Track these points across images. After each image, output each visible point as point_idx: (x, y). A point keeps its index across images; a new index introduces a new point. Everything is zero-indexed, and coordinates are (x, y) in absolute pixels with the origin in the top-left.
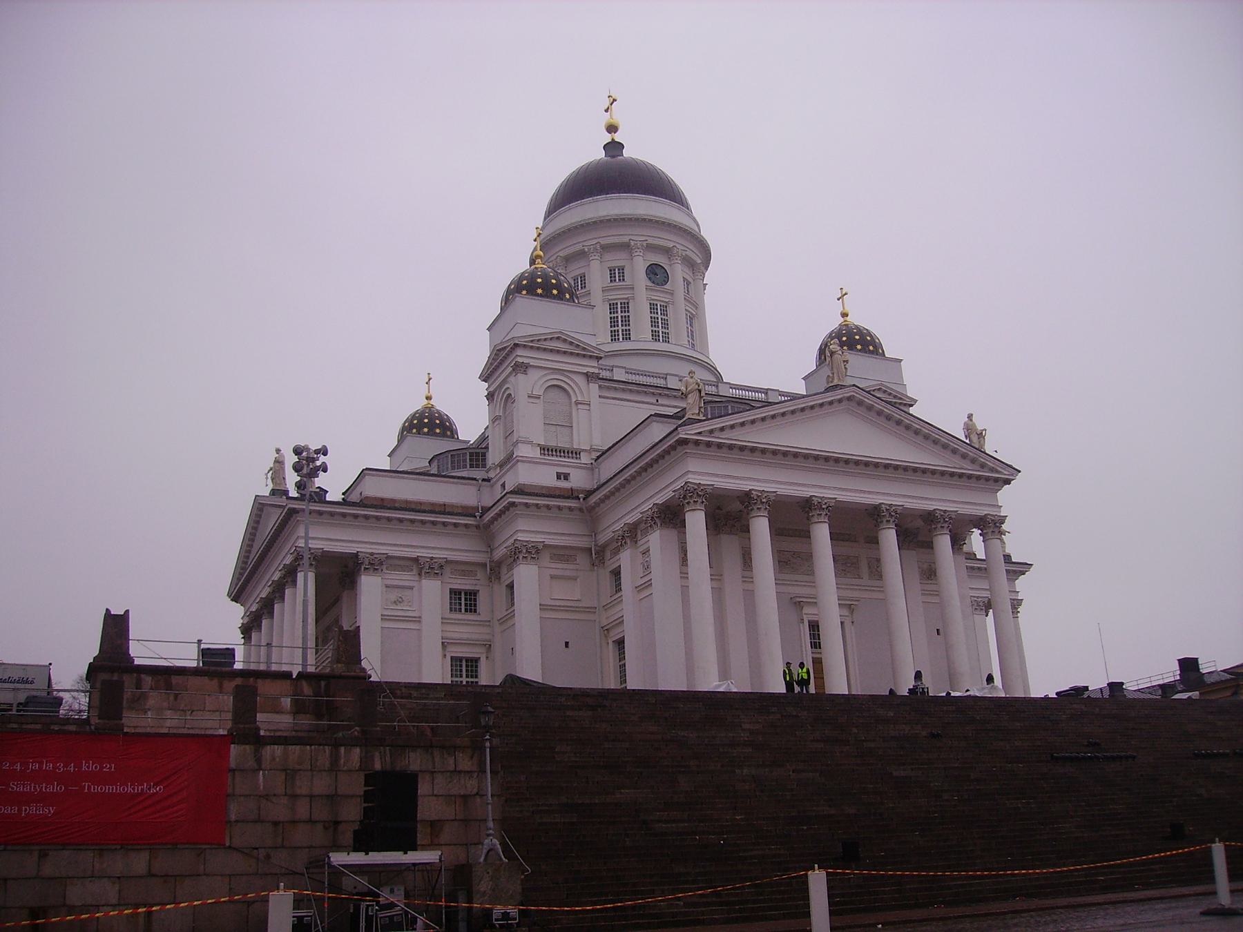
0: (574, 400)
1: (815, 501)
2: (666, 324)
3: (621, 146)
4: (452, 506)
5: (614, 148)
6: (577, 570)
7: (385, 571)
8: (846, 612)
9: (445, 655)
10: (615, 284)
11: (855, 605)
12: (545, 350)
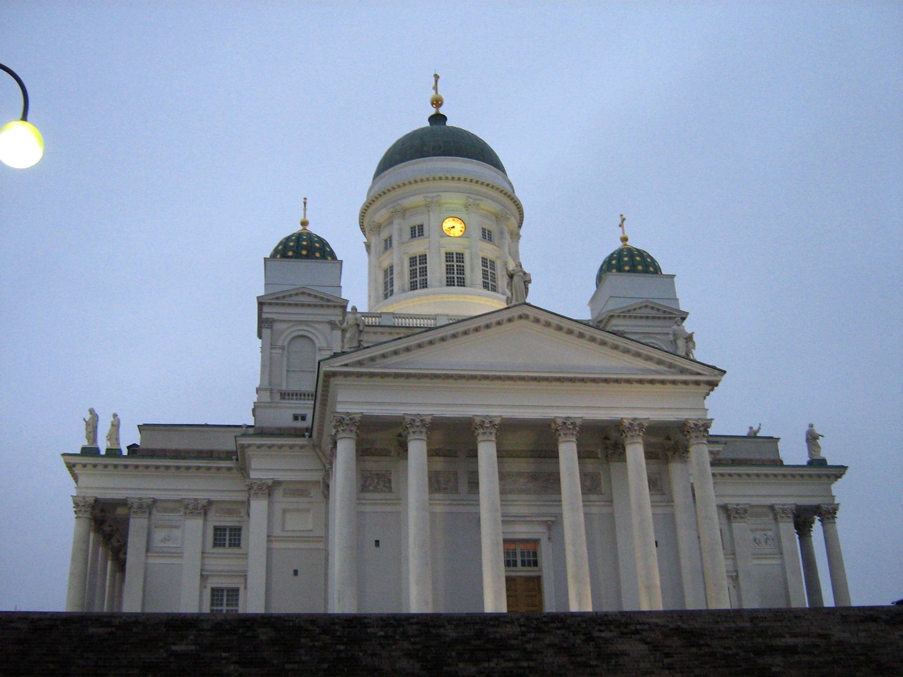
0: (317, 347)
2: (461, 270)
3: (443, 118)
4: (220, 452)
5: (438, 119)
6: (290, 502)
7: (154, 512)
9: (205, 587)
11: (553, 522)
12: (290, 305)
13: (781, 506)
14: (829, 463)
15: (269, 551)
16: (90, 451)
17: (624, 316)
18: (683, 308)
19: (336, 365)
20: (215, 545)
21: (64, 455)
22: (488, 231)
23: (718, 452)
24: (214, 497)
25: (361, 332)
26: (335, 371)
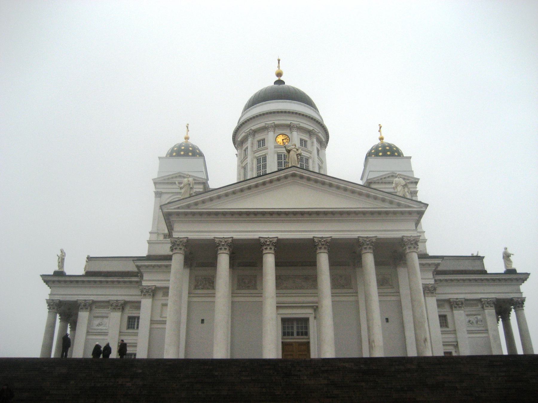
1: (262, 240)
3: (282, 82)
8: (310, 311)
10: (261, 148)
13: (486, 300)
14: (518, 271)
15: (151, 329)
16: (59, 274)
17: (378, 183)
18: (416, 176)
19: (171, 208)
20: (128, 328)
21: (42, 276)
22: (304, 141)
23: (438, 264)
24: (127, 298)
25: (191, 188)
26: (171, 212)
